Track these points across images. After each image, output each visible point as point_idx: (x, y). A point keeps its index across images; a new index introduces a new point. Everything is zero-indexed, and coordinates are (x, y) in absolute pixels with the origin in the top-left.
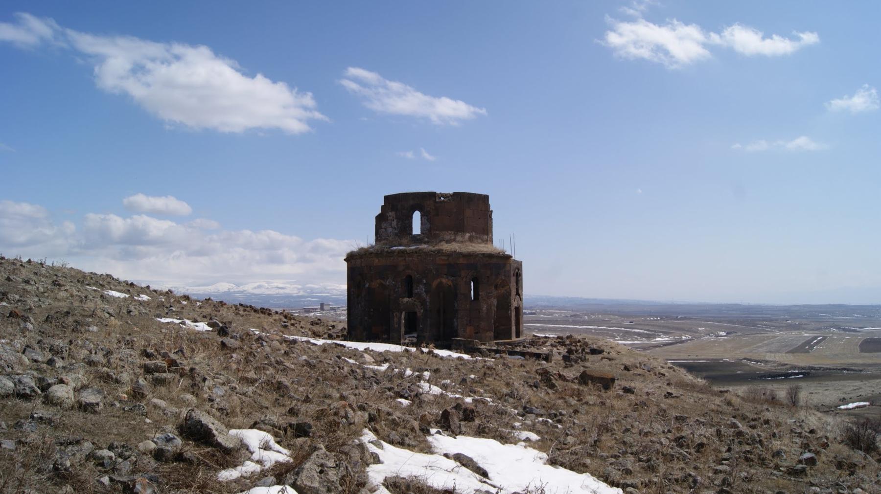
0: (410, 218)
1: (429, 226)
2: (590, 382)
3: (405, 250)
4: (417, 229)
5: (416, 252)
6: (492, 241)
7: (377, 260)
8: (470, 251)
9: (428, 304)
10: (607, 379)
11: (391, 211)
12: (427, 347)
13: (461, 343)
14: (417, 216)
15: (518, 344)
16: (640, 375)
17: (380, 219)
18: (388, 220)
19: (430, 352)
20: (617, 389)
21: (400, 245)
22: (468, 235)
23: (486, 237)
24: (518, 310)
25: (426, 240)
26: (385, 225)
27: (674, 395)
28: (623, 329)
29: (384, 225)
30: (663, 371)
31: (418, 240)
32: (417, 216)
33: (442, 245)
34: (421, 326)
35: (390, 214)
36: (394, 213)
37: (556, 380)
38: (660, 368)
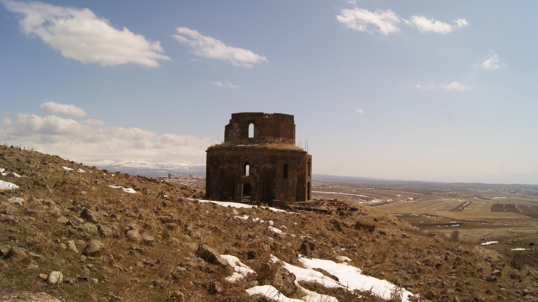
1: (259, 133)
2: (362, 228)
3: (245, 146)
4: (251, 134)
5: (252, 148)
6: (295, 143)
7: (228, 153)
8: (283, 148)
9: (258, 179)
10: (371, 226)
11: (236, 123)
12: (264, 206)
13: (278, 203)
14: (251, 127)
15: (309, 204)
16: (384, 224)
17: (228, 128)
18: (233, 128)
19: (267, 209)
20: (375, 233)
21: (242, 144)
22: (281, 139)
23: (291, 140)
24: (309, 184)
25: (257, 141)
26: (232, 131)
27: (407, 236)
28: (352, 194)
29: (231, 131)
30: (395, 222)
31: (252, 141)
32: (251, 127)
33: (267, 145)
34: (253, 192)
35: (235, 124)
36: (237, 124)
37: (342, 226)
38: (393, 220)
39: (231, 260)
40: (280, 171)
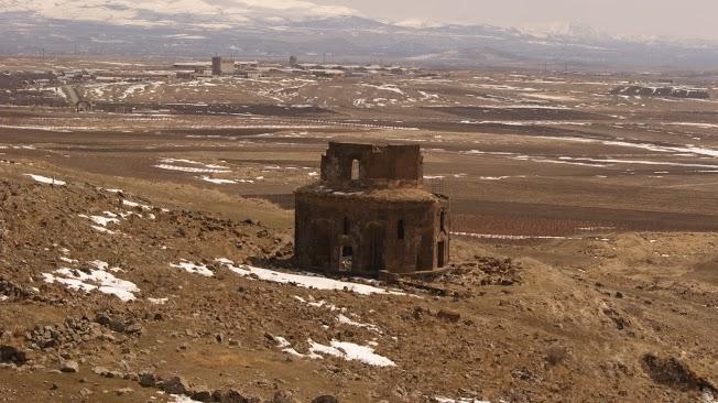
0: (350, 165)
5: (353, 198)
22: (398, 181)
39: (281, 339)
40: (392, 228)
